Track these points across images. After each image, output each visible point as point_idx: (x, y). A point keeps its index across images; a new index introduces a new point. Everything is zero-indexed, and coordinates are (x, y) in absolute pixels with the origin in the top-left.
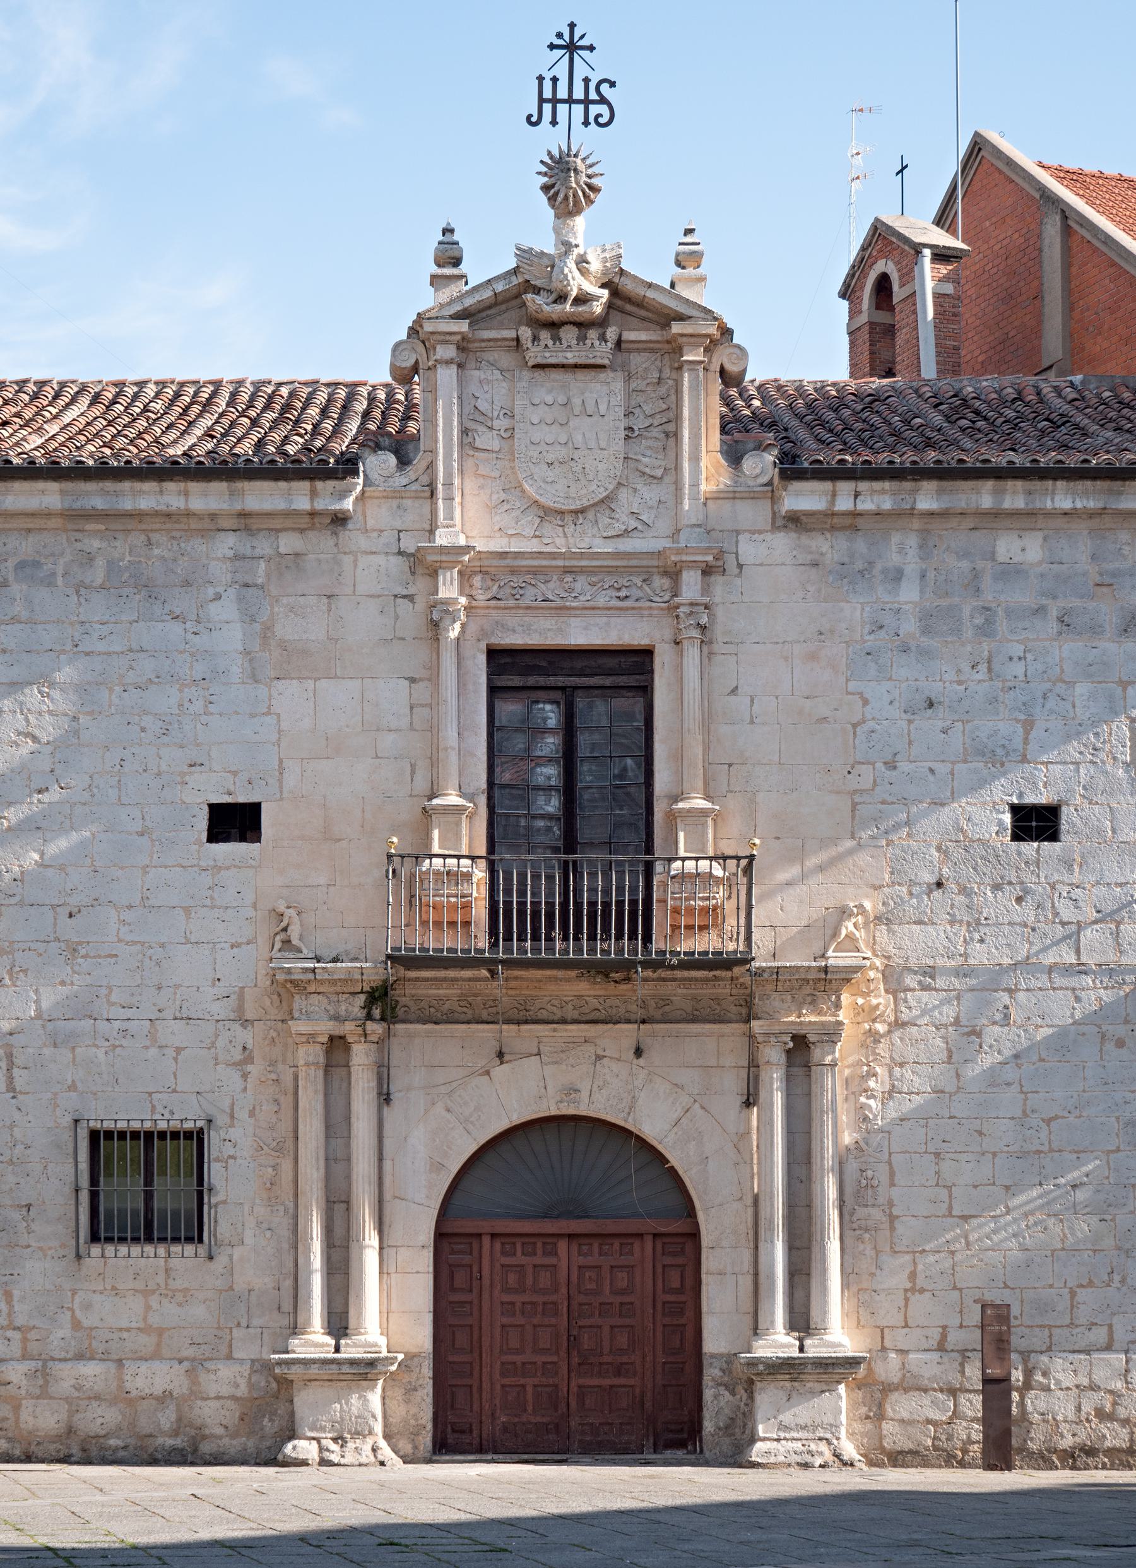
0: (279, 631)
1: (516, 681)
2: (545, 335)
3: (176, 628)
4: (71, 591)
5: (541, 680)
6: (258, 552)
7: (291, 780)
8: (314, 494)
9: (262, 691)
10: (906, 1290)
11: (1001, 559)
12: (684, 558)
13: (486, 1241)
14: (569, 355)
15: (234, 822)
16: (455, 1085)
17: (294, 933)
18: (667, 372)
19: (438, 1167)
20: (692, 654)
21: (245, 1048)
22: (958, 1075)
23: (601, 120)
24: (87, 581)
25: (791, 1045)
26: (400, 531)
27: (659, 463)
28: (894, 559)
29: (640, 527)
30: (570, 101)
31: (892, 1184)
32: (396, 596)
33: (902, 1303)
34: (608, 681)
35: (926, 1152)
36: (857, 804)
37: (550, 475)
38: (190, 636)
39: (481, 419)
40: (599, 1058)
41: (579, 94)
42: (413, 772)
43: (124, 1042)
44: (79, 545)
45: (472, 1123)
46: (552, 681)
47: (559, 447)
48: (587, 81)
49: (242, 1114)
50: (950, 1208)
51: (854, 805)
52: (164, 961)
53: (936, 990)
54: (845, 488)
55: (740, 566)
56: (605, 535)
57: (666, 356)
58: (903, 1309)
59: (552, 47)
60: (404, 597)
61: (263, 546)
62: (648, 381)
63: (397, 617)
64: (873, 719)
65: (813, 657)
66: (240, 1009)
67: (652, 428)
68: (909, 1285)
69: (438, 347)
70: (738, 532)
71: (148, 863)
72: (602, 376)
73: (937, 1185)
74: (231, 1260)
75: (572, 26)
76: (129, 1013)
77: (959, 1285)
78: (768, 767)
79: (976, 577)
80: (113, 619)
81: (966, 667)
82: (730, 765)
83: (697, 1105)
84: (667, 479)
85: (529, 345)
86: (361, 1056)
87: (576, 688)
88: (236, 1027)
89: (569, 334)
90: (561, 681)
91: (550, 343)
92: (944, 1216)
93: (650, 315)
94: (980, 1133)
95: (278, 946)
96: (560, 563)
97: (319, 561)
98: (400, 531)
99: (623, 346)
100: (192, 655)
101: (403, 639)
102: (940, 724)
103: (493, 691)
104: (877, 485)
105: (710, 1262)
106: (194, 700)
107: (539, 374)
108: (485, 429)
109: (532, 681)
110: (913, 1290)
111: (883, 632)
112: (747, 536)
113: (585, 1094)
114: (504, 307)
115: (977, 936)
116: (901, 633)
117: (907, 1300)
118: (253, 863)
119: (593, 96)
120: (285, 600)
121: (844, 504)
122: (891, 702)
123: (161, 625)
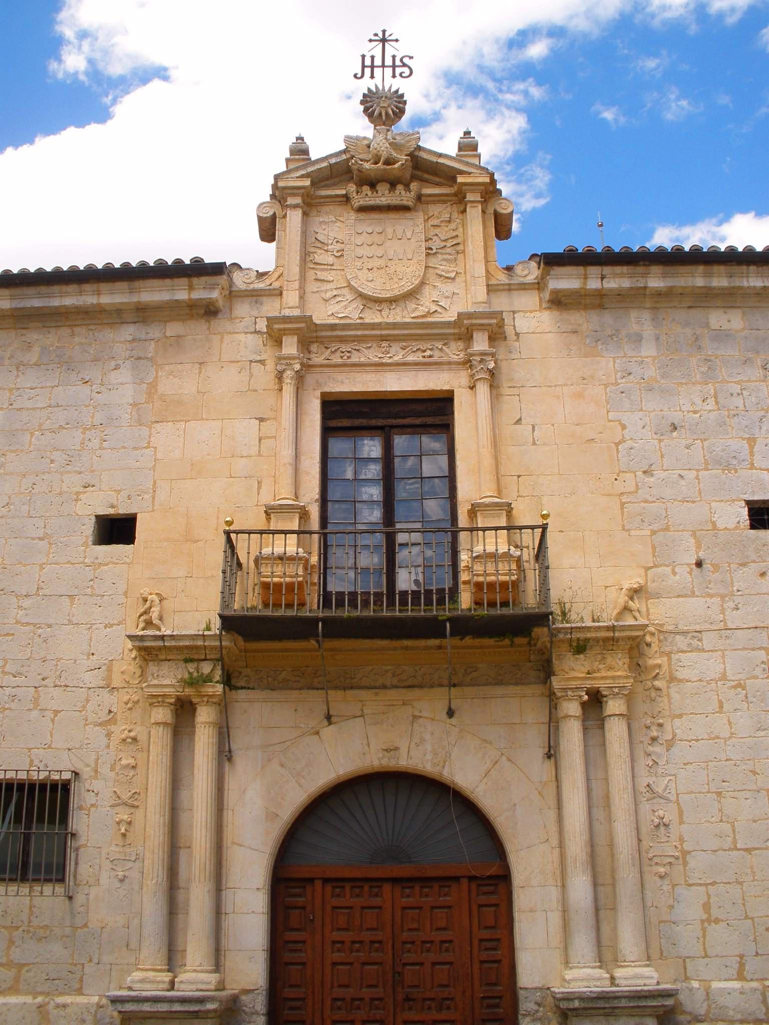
0: (161, 389)
1: (346, 423)
2: (366, 189)
3: (86, 389)
4: (13, 368)
5: (363, 422)
6: (150, 336)
7: (161, 495)
8: (191, 288)
9: (145, 431)
10: (702, 921)
11: (713, 327)
12: (474, 321)
13: (318, 884)
14: (383, 199)
15: (117, 530)
16: (288, 743)
17: (155, 614)
18: (455, 215)
19: (272, 816)
20: (483, 389)
21: (110, 712)
22: (730, 723)
24: (25, 362)
25: (586, 697)
28: (634, 328)
29: (439, 310)
31: (681, 822)
32: (251, 361)
33: (700, 934)
34: (418, 421)
35: (708, 792)
36: (625, 503)
37: (370, 275)
38: (94, 395)
39: (319, 245)
40: (415, 717)
41: (388, 62)
42: (259, 488)
43: (13, 705)
44: (23, 338)
45: (303, 777)
46: (374, 422)
47: (377, 259)
48: (394, 57)
49: (105, 770)
50: (735, 841)
51: (623, 504)
52: (50, 639)
53: (703, 650)
54: (594, 270)
55: (517, 334)
58: (702, 939)
59: (371, 41)
60: (259, 361)
61: (154, 332)
63: (251, 375)
64: (631, 439)
65: (579, 396)
66: (109, 678)
68: (705, 917)
69: (289, 199)
70: (514, 312)
71: (45, 561)
72: (408, 215)
73: (721, 821)
74: (88, 899)
75: (384, 32)
76: (19, 680)
77: (750, 915)
78: (550, 477)
79: (697, 339)
80: (40, 386)
81: (698, 401)
82: (519, 476)
83: (504, 758)
84: (458, 280)
85: (354, 194)
86: (205, 715)
87: (392, 427)
88: (105, 693)
89: (383, 188)
90: (380, 422)
91: (369, 193)
92: (730, 850)
94: (754, 773)
95: (142, 625)
96: (378, 332)
97: (195, 340)
99: (423, 199)
100: (95, 407)
101: (256, 391)
102: (684, 442)
103: (327, 432)
104: (618, 269)
105: (522, 900)
106: (92, 440)
107: (362, 216)
109: (357, 422)
110: (709, 921)
111: (631, 377)
112: (522, 314)
113: (404, 751)
114: (337, 180)
115: (731, 605)
116: (645, 377)
117: (704, 930)
118: (128, 560)
119: (398, 63)
120: (167, 368)
121: (594, 284)
122: (644, 427)
123: (74, 388)
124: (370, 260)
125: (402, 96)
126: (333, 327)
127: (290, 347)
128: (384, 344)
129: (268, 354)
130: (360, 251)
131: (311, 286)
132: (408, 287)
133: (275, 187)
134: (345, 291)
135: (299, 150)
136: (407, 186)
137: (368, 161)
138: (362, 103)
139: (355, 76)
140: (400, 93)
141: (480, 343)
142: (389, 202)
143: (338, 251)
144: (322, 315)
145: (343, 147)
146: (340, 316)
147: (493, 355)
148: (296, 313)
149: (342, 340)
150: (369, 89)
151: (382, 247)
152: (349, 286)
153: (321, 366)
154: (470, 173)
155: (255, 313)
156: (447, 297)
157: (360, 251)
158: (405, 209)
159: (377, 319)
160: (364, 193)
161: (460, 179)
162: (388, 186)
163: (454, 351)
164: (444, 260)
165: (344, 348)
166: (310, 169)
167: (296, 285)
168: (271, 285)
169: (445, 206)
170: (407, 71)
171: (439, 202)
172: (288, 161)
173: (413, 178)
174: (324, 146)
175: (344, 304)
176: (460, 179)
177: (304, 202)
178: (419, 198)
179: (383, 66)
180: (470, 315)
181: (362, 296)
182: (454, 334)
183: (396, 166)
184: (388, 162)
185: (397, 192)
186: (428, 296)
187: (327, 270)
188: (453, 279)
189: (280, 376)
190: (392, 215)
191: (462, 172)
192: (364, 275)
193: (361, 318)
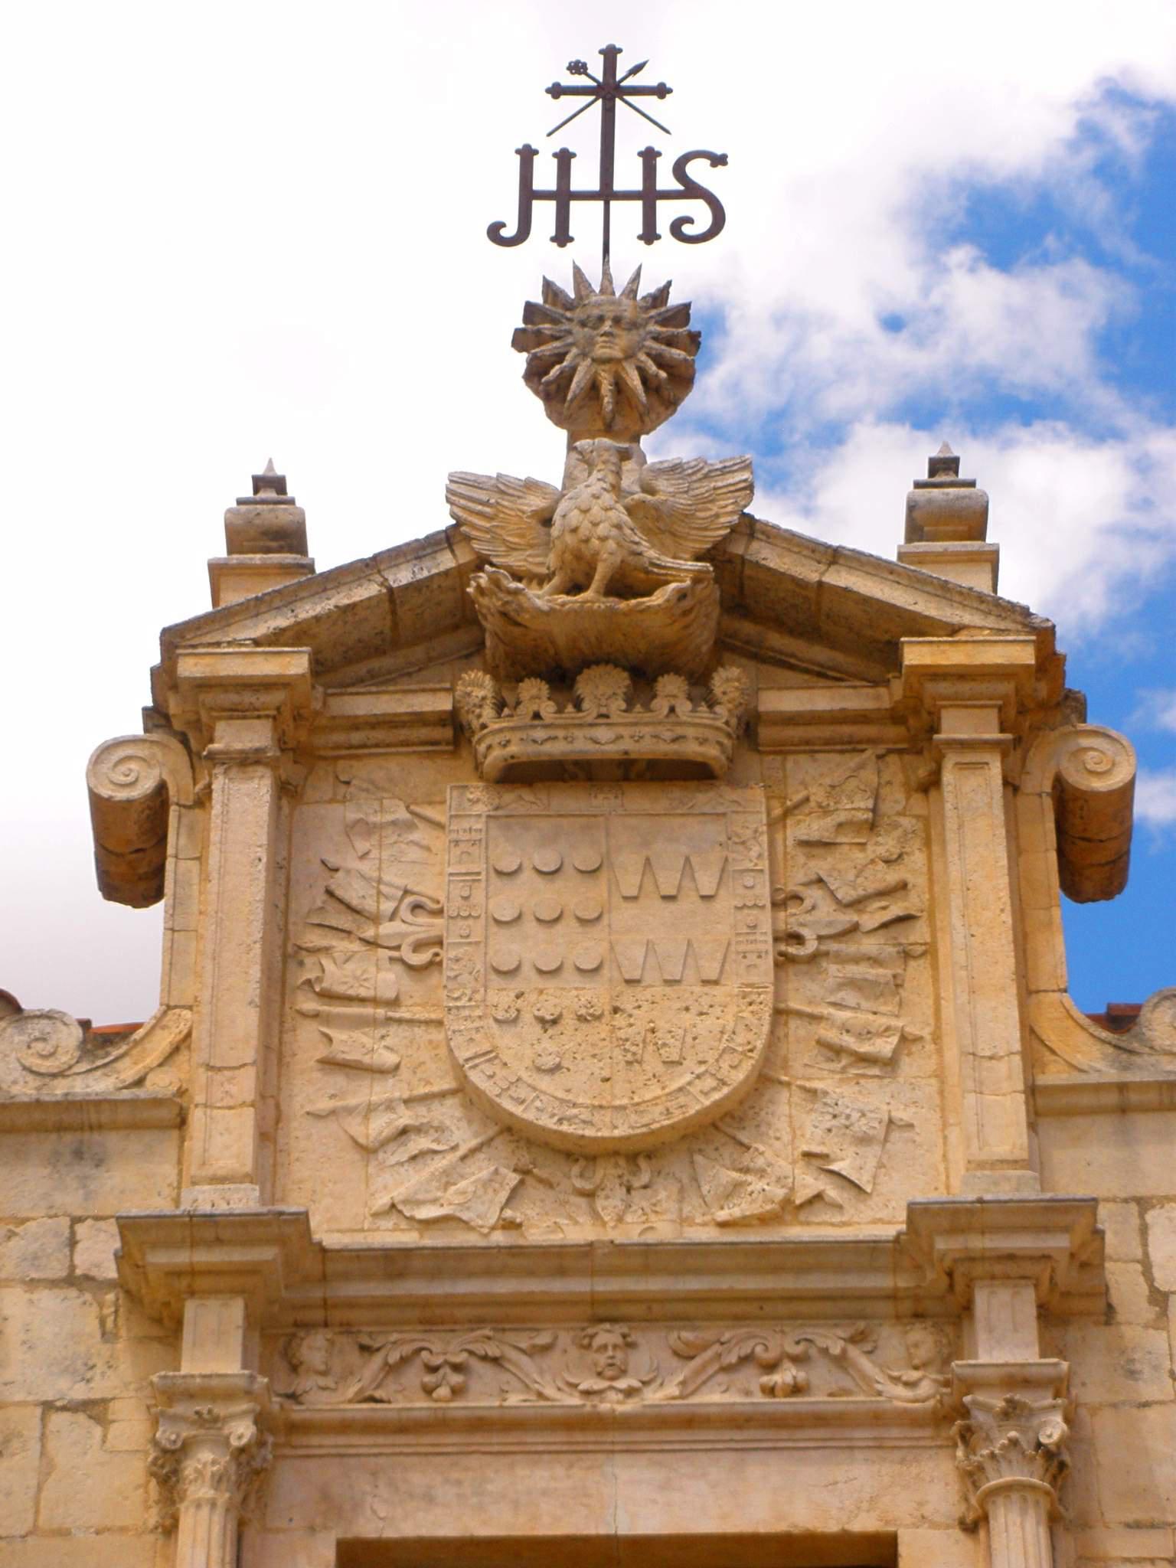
2: (534, 693)
14: (603, 733)
18: (895, 799)
23: (687, 229)
26: (76, 1220)
27: (883, 1021)
29: (832, 1193)
30: (606, 193)
32: (48, 1407)
37: (549, 1047)
39: (344, 921)
41: (628, 175)
47: (576, 980)
48: (649, 157)
56: (723, 1215)
57: (893, 759)
59: (556, 91)
62: (842, 817)
63: (47, 1466)
67: (858, 935)
69: (221, 728)
70: (1143, 1204)
72: (704, 799)
75: (610, 55)
84: (908, 1066)
85: (488, 712)
89: (602, 688)
91: (548, 709)
93: (839, 658)
96: (578, 1286)
98: (76, 1220)
99: (765, 733)
108: (356, 946)
114: (419, 652)
119: (666, 180)
124: (550, 984)
125: (683, 313)
126: (393, 1262)
127: (215, 1348)
128: (606, 1335)
129: (120, 1376)
130: (507, 948)
131: (310, 1091)
132: (703, 1098)
133: (164, 678)
134: (448, 1112)
135: (266, 529)
136: (699, 682)
137: (542, 580)
138: (520, 341)
139: (494, 232)
140: (674, 299)
141: (1005, 1338)
142: (627, 745)
143: (418, 947)
144: (348, 1208)
145: (443, 520)
146: (425, 1213)
147: (1059, 1386)
148: (244, 1200)
149: (434, 1317)
150: (549, 287)
151: (597, 931)
152: (464, 1091)
153: (345, 1427)
154: (954, 630)
155: (71, 1200)
156: (864, 1140)
157: (507, 948)
158: (692, 773)
159: (578, 1231)
160: (527, 709)
161: (916, 654)
162: (621, 680)
163: (895, 1374)
164: (852, 983)
165: (444, 1347)
166: (307, 610)
167: (245, 1085)
168: (139, 1082)
169: (853, 761)
170: (700, 213)
171: (831, 745)
172: (218, 572)
173: (725, 647)
174: (366, 515)
175: (440, 1163)
176: (916, 654)
177: (281, 742)
178: (749, 729)
179: (606, 193)
180: (959, 1217)
181: (512, 1133)
182: (893, 1296)
183: (658, 599)
184: (626, 584)
185: (661, 705)
186: (790, 1130)
187: (374, 1022)
188: (890, 1064)
189: (167, 1471)
190: (639, 800)
191: (920, 626)
192: (521, 1047)
193: (510, 1225)
